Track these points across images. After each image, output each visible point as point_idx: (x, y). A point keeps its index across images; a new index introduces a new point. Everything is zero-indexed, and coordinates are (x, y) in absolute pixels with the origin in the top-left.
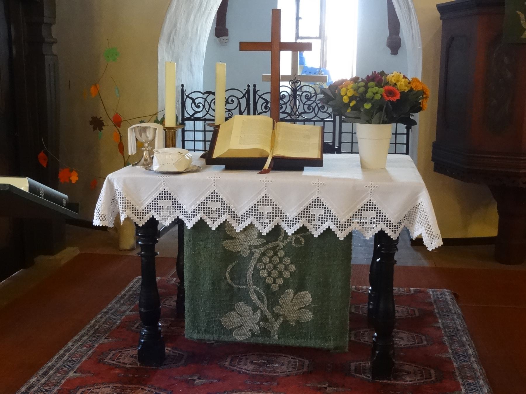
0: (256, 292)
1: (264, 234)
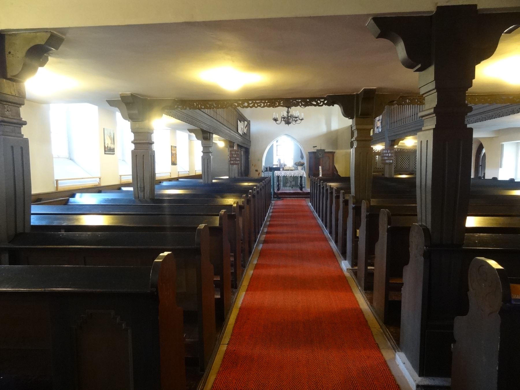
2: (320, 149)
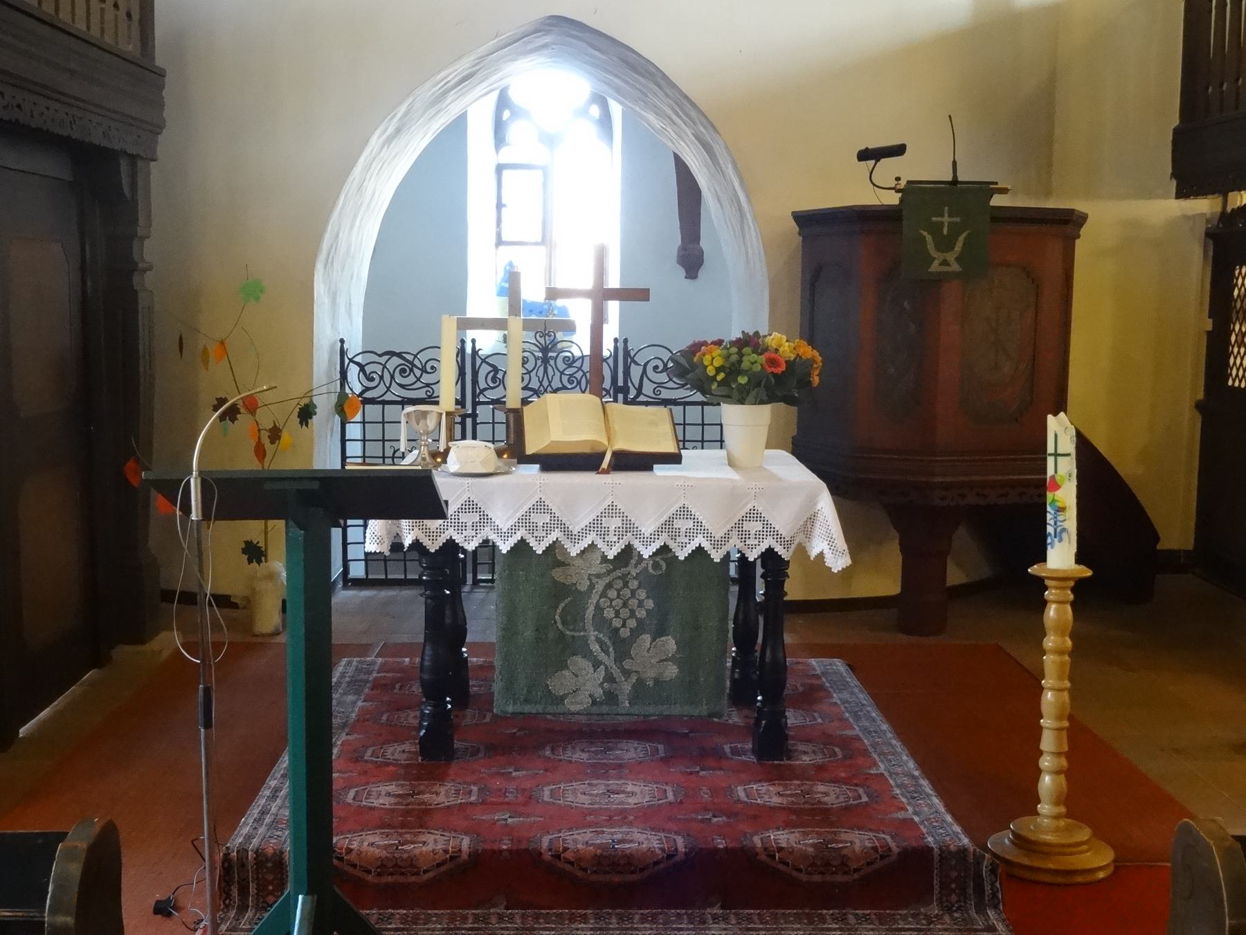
0: (598, 640)
1: (611, 557)
2: (949, 178)
